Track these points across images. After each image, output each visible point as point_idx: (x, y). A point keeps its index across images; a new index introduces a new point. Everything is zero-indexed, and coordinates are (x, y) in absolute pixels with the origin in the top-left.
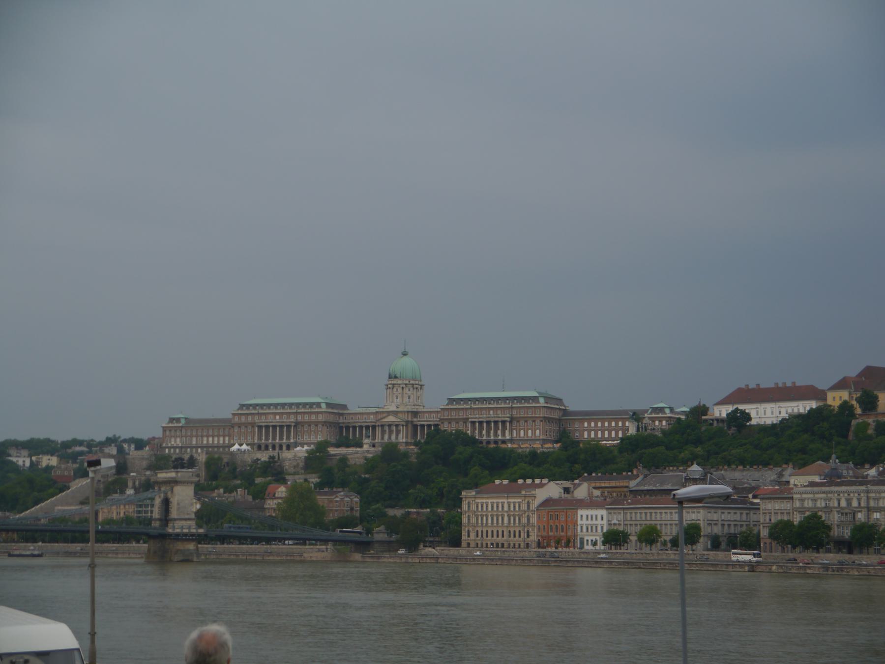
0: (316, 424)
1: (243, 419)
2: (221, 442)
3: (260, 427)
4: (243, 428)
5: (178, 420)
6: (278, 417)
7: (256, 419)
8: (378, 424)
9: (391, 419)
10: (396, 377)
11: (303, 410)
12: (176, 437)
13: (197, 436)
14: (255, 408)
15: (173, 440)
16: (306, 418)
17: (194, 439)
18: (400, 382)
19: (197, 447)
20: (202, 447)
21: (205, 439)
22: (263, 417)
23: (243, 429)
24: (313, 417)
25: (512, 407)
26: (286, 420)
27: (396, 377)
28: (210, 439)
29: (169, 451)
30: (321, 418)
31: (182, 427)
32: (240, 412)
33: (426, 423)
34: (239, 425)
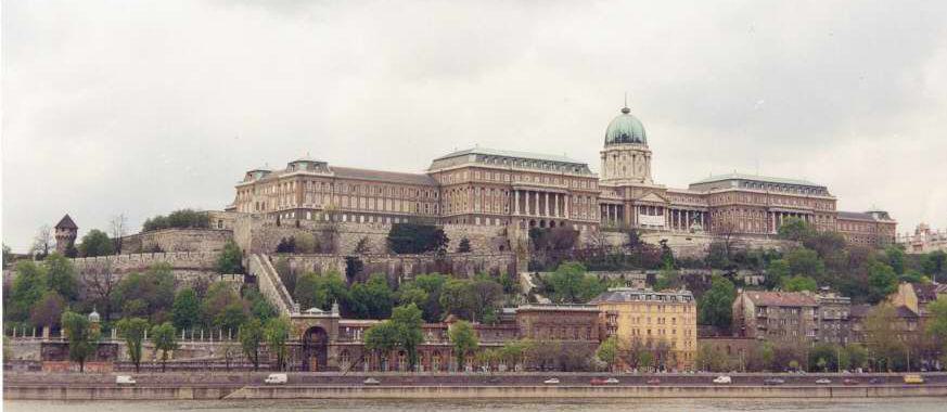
0: (589, 195)
1: (488, 177)
2: (371, 207)
3: (522, 192)
4: (488, 190)
5: (320, 165)
7: (507, 179)
8: (636, 203)
9: (652, 198)
10: (638, 141)
11: (570, 174)
16: (575, 185)
19: (358, 214)
22: (517, 177)
23: (488, 192)
24: (584, 186)
26: (547, 184)
27: (638, 141)
30: (593, 187)
31: (334, 178)
33: (681, 208)
34: (483, 186)
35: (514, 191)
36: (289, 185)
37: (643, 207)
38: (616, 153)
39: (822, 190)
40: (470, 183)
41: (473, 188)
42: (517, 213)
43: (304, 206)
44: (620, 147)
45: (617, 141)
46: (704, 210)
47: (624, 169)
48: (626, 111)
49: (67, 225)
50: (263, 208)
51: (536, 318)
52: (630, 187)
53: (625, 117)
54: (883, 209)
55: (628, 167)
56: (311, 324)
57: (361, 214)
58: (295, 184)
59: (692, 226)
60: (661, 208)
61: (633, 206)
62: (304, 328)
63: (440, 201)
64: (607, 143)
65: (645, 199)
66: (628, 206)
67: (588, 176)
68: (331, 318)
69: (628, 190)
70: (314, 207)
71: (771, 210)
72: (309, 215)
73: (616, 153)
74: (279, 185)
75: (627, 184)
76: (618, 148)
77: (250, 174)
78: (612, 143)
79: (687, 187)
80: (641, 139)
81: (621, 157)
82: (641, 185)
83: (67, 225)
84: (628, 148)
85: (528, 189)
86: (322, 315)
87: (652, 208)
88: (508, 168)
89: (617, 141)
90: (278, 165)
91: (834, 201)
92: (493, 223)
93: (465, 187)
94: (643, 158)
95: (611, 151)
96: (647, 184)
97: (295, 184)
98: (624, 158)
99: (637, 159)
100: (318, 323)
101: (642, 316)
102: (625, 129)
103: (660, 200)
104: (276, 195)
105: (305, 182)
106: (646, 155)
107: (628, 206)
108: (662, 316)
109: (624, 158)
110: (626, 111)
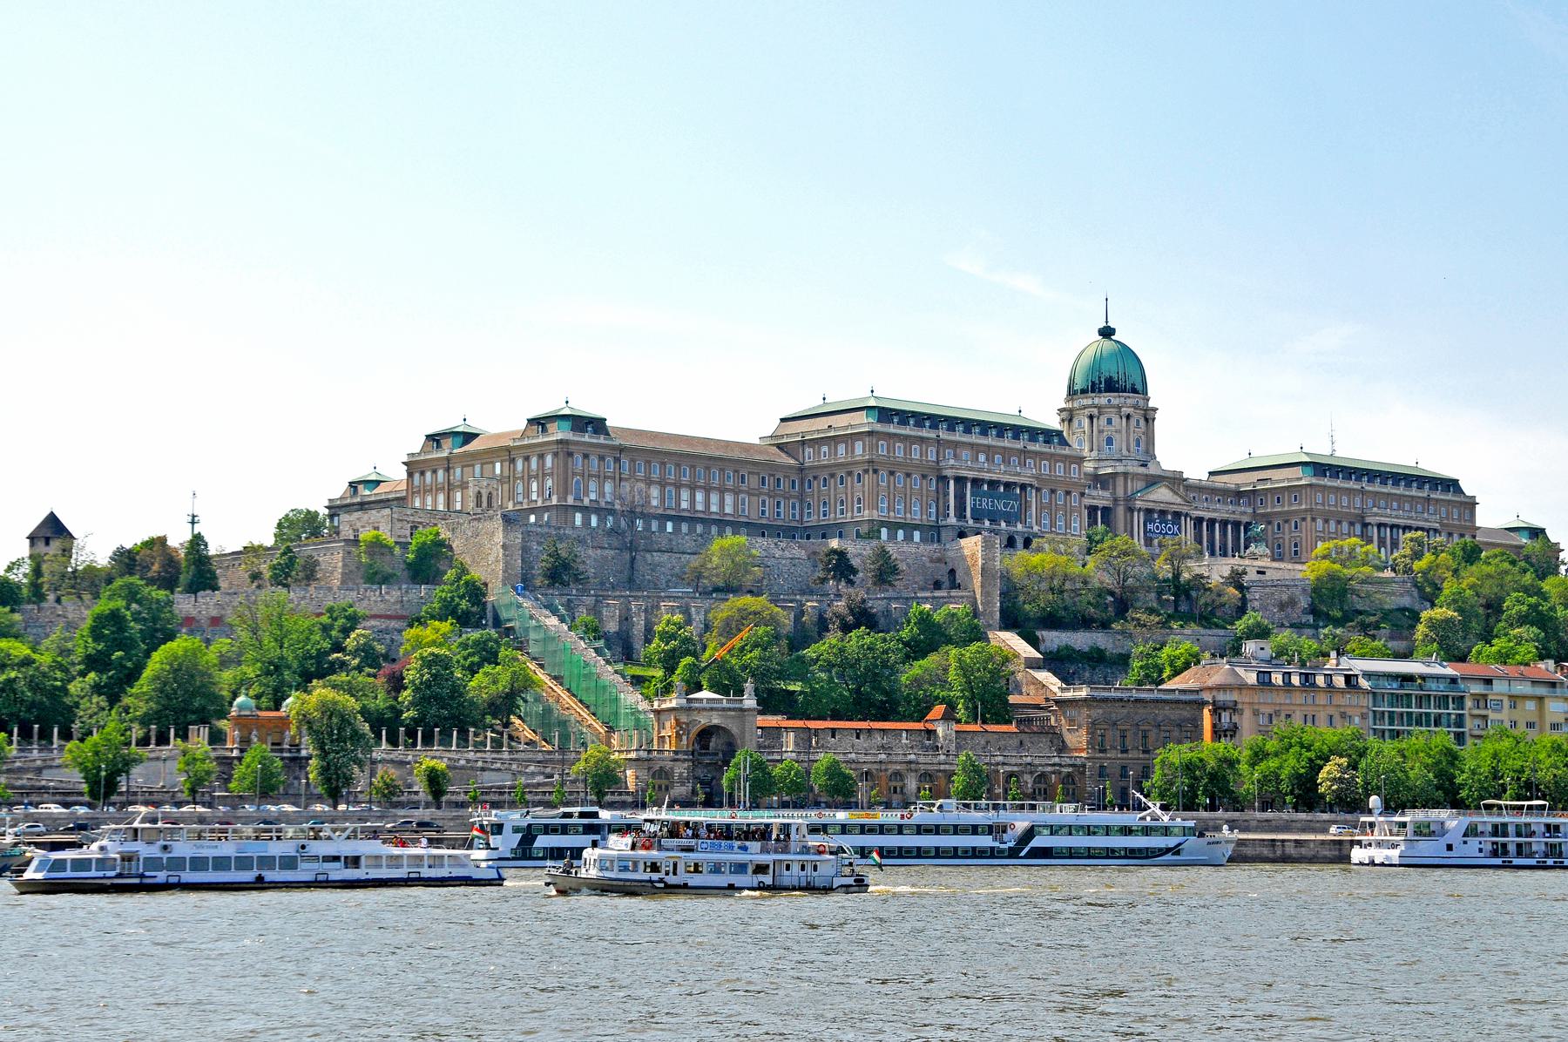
5: (597, 425)
6: (982, 458)
8: (1139, 504)
12: (601, 478)
13: (662, 484)
14: (934, 426)
15: (593, 485)
17: (655, 492)
18: (1141, 403)
20: (678, 519)
21: (685, 495)
25: (1428, 499)
27: (1134, 391)
28: (714, 498)
29: (586, 522)
32: (892, 429)
33: (1207, 515)
35: (943, 479)
36: (534, 461)
37: (1149, 511)
38: (1095, 411)
39: (1452, 485)
40: (870, 462)
41: (875, 471)
42: (952, 520)
43: (570, 500)
44: (1103, 399)
45: (1093, 388)
46: (1245, 519)
47: (1110, 441)
48: (1107, 332)
49: (52, 530)
50: (490, 505)
51: (1097, 712)
52: (1125, 474)
53: (1107, 344)
54: (1537, 523)
55: (1116, 437)
56: (703, 720)
57: (670, 518)
58: (549, 460)
59: (1252, 548)
60: (1177, 515)
61: (1131, 510)
62: (695, 730)
63: (801, 498)
64: (1072, 393)
65: (1152, 497)
66: (1120, 511)
67: (1067, 451)
68: (742, 710)
69: (1120, 481)
70: (586, 502)
71: (1368, 520)
72: (578, 518)
73: (1095, 411)
74: (512, 461)
75: (1120, 469)
76: (1096, 401)
77: (435, 439)
78: (1084, 391)
79: (1205, 477)
80: (1139, 387)
81: (1103, 420)
82: (1142, 470)
83: (52, 530)
84: (1115, 402)
85: (971, 474)
86: (725, 704)
87: (1163, 513)
88: (932, 435)
89: (1093, 388)
90: (500, 418)
91: (1471, 504)
92: (909, 538)
93: (858, 470)
94: (1142, 422)
95: (1085, 407)
96: (1152, 470)
97: (549, 460)
98: (1109, 421)
99: (1133, 422)
100: (716, 720)
101: (1277, 713)
102: (1110, 370)
103: (1179, 500)
104: (502, 480)
105: (570, 454)
106: (1148, 416)
107: (1120, 511)
108: (1310, 711)
109: (1109, 421)
110: (1107, 332)
